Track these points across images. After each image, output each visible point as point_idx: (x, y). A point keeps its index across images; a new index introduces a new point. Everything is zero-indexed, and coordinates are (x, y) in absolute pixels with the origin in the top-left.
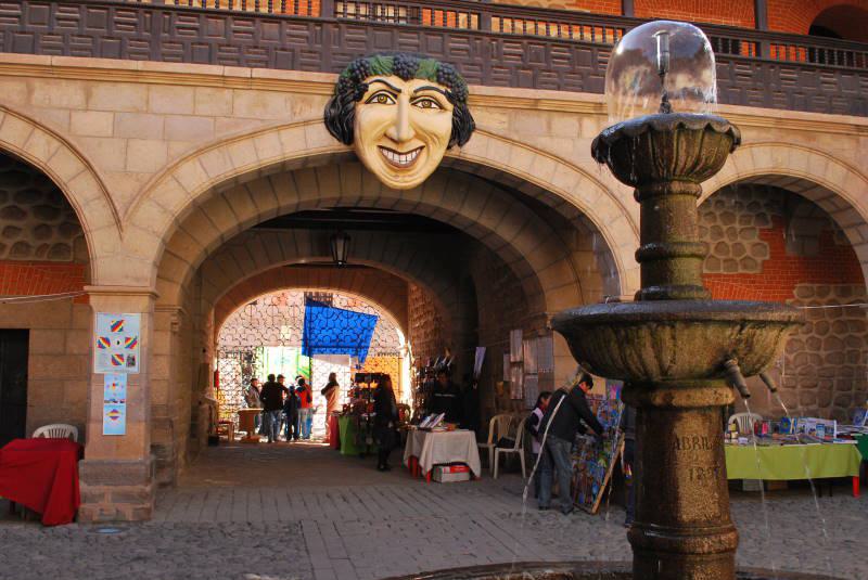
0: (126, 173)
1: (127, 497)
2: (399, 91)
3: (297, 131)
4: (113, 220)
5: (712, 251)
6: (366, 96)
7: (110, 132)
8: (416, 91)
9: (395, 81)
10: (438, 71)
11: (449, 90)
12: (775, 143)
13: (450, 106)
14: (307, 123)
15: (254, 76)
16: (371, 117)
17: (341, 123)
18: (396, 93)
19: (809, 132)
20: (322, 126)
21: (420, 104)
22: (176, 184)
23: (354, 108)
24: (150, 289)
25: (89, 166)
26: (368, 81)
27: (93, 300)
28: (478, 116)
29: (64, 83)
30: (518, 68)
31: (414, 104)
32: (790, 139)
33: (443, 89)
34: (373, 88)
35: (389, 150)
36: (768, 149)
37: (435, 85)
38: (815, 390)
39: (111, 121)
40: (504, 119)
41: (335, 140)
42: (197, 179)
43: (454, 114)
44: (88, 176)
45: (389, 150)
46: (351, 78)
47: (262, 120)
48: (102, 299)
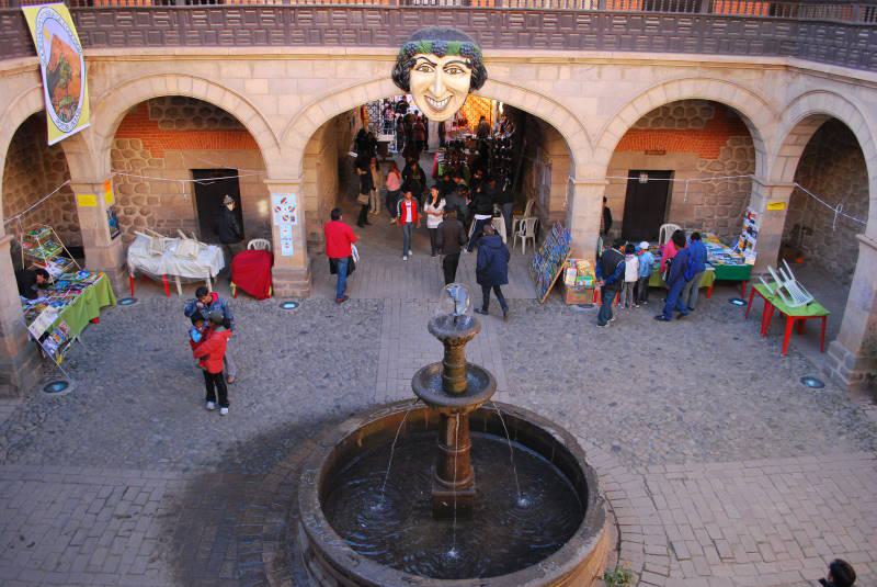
1: (298, 286)
3: (378, 83)
4: (273, 142)
5: (671, 114)
6: (416, 67)
9: (433, 58)
11: (469, 61)
12: (699, 78)
13: (469, 71)
14: (381, 79)
16: (417, 78)
17: (402, 80)
18: (434, 65)
19: (726, 68)
20: (391, 82)
23: (408, 73)
27: (270, 188)
28: (491, 70)
30: (520, 31)
32: (710, 74)
33: (464, 60)
34: (419, 62)
36: (692, 82)
37: (458, 58)
38: (729, 206)
40: (508, 70)
42: (321, 115)
44: (258, 118)
48: (274, 187)
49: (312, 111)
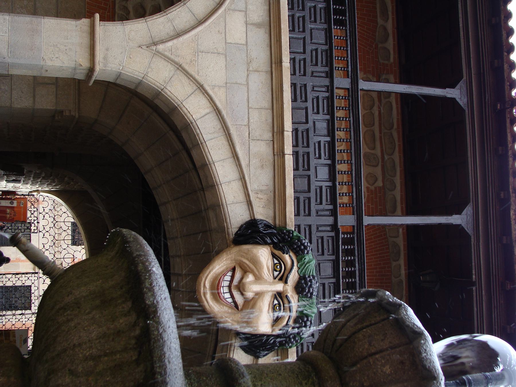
0: (197, 52)
2: (286, 282)
3: (241, 197)
6: (277, 252)
7: (229, 41)
8: (287, 296)
9: (293, 277)
10: (307, 316)
14: (249, 203)
15: (286, 156)
21: (276, 302)
22: (190, 93)
23: (265, 243)
24: (98, 68)
25: (201, 22)
26: (291, 254)
27: (85, 22)
29: (267, 8)
31: (275, 297)
34: (287, 257)
35: (233, 277)
39: (240, 42)
41: (236, 230)
43: (269, 336)
44: (193, 23)
45: (233, 277)
46: (292, 238)
47: (249, 165)
49: (203, 101)
